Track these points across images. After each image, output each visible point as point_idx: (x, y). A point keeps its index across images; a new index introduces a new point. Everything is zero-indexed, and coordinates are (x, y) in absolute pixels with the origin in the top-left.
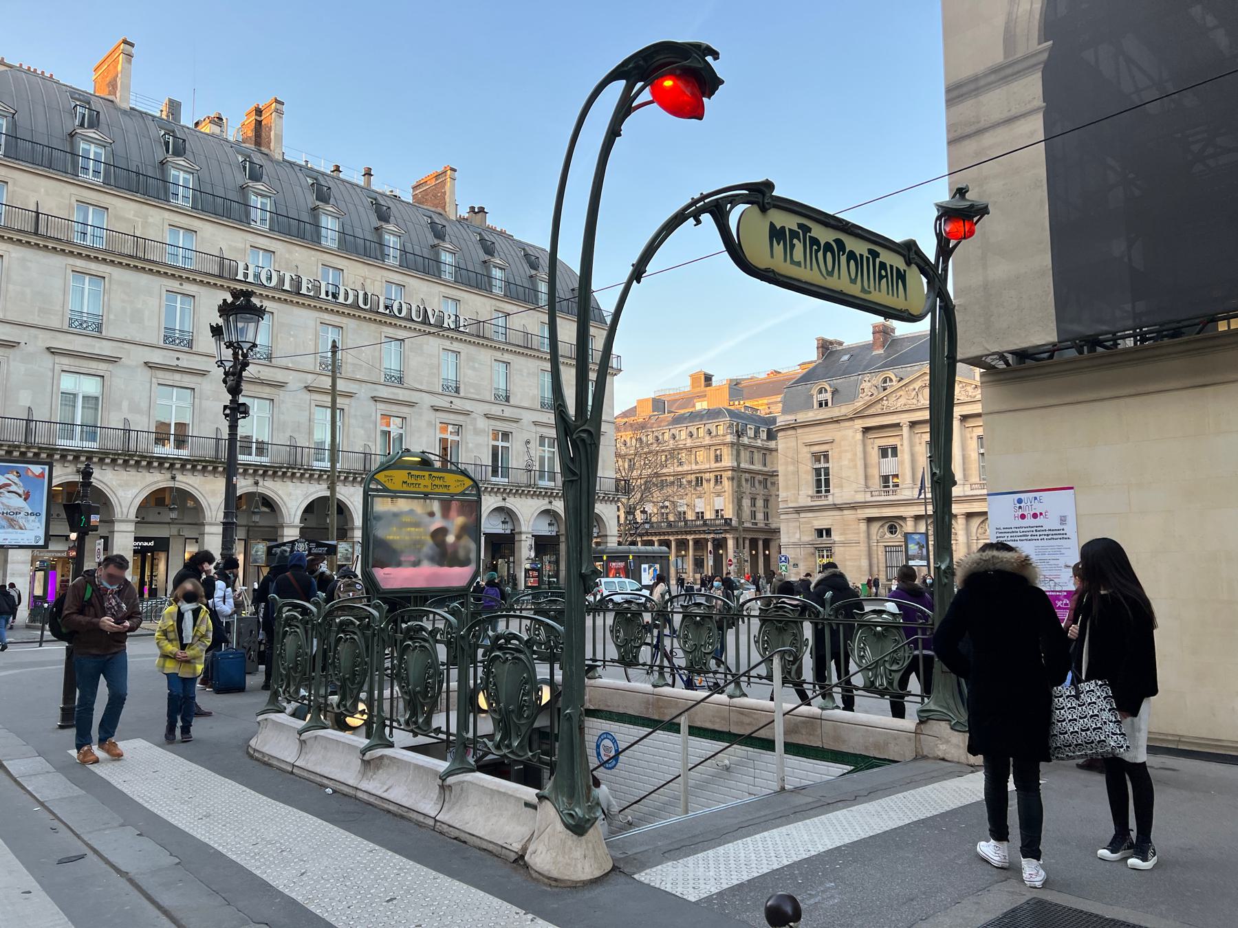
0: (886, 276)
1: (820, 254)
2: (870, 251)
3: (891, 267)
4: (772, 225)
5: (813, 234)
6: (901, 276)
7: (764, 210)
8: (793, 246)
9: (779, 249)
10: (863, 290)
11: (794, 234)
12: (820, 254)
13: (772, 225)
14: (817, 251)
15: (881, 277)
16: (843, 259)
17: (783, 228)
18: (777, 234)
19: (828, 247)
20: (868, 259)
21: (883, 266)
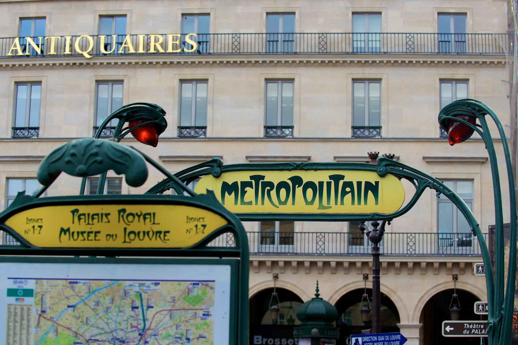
0: (352, 191)
1: (273, 193)
3: (359, 184)
4: (225, 185)
5: (266, 180)
8: (244, 193)
10: (321, 206)
11: (245, 184)
12: (273, 193)
13: (225, 185)
14: (269, 191)
15: (344, 193)
16: (299, 190)
19: (283, 185)
20: (329, 184)
21: (350, 184)
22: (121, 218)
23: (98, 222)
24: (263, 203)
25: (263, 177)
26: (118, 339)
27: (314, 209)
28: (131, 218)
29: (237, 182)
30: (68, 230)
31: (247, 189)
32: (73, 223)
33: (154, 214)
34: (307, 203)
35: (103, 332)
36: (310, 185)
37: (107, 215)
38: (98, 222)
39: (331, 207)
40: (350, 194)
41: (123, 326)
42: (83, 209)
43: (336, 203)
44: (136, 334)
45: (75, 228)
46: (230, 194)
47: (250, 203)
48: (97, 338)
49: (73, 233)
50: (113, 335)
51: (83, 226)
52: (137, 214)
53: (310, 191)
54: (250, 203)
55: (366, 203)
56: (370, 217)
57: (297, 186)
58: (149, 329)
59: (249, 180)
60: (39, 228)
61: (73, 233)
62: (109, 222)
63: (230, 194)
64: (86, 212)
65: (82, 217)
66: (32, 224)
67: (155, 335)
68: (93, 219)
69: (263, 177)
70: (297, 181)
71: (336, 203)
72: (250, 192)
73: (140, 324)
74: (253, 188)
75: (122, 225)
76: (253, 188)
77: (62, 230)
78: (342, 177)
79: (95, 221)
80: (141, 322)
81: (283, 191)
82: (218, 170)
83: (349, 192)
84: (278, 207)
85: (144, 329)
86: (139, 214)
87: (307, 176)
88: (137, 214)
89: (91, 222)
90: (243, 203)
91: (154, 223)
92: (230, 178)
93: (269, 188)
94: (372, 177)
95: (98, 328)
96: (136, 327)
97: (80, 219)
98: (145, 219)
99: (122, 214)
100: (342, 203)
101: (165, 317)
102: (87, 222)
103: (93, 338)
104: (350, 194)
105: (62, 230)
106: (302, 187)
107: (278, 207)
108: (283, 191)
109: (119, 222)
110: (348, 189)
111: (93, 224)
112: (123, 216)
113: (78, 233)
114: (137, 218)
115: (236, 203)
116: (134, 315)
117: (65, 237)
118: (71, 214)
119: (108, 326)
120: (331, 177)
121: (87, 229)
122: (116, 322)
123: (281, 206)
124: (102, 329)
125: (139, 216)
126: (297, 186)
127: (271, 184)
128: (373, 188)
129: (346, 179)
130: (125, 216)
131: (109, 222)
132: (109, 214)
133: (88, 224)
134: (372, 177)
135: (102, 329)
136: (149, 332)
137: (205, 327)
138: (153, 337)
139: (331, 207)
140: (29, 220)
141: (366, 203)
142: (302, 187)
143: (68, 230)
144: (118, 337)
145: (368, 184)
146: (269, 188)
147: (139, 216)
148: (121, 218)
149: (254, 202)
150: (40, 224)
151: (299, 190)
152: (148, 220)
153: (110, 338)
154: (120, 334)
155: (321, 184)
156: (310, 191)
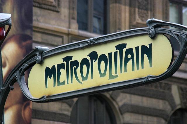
0: (132, 58)
1: (78, 70)
2: (117, 47)
3: (137, 48)
5: (73, 59)
6: (147, 51)
7: (41, 63)
8: (59, 74)
9: (51, 80)
10: (111, 77)
11: (61, 66)
12: (78, 70)
14: (75, 69)
15: (127, 60)
16: (95, 64)
17: (54, 66)
18: (49, 72)
19: (85, 61)
20: (116, 53)
21: (130, 51)
24: (72, 82)
25: (71, 58)
27: (105, 81)
29: (54, 66)
31: (62, 70)
34: (102, 75)
36: (103, 57)
39: (117, 76)
40: (131, 60)
43: (121, 72)
46: (50, 78)
47: (63, 83)
53: (103, 63)
54: (63, 83)
55: (143, 67)
56: (145, 80)
57: (94, 60)
59: (61, 62)
63: (50, 78)
69: (71, 58)
70: (93, 55)
71: (121, 72)
72: (63, 71)
74: (65, 69)
76: (65, 69)
78: (124, 45)
81: (85, 67)
82: (39, 58)
83: (130, 59)
84: (81, 83)
87: (101, 51)
90: (59, 84)
92: (50, 63)
93: (75, 67)
94: (145, 41)
100: (126, 71)
104: (131, 60)
106: (97, 61)
107: (81, 83)
108: (85, 67)
110: (129, 56)
115: (54, 85)
120: (117, 47)
123: (84, 82)
126: (94, 60)
127: (76, 63)
128: (147, 51)
129: (128, 47)
134: (145, 41)
139: (117, 76)
141: (143, 67)
142: (97, 61)
145: (144, 47)
146: (75, 67)
149: (66, 82)
151: (95, 64)
155: (110, 54)
156: (103, 63)
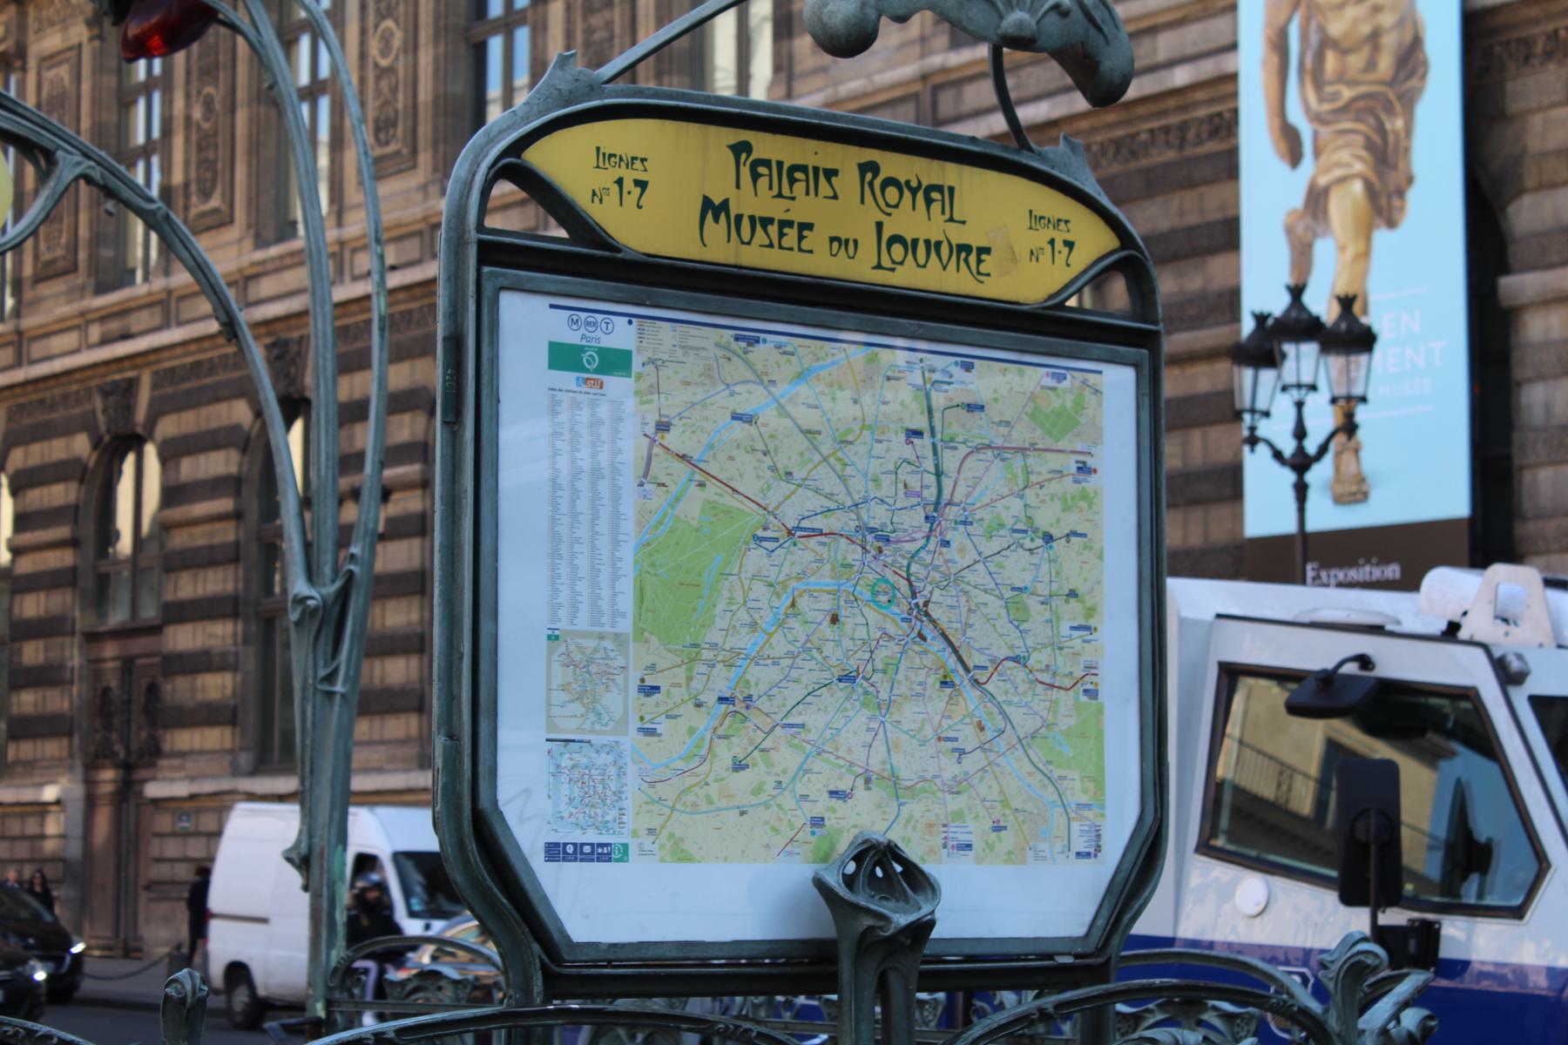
22: (867, 188)
23: (807, 193)
26: (872, 530)
28: (892, 193)
30: (725, 205)
32: (738, 186)
33: (951, 190)
35: (833, 506)
37: (831, 174)
38: (807, 193)
41: (886, 489)
42: (766, 146)
44: (918, 517)
45: (753, 200)
48: (818, 523)
49: (739, 218)
50: (859, 517)
51: (753, 200)
52: (908, 182)
58: (949, 503)
60: (638, 190)
61: (739, 218)
62: (835, 197)
64: (774, 157)
65: (762, 170)
66: (616, 173)
67: (965, 523)
68: (792, 181)
73: (928, 487)
75: (872, 213)
77: (707, 204)
79: (799, 188)
80: (931, 479)
85: (937, 503)
86: (914, 184)
88: (908, 182)
89: (786, 191)
91: (951, 219)
95: (817, 491)
96: (919, 495)
97: (755, 177)
98: (929, 202)
99: (869, 176)
101: (987, 469)
102: (775, 191)
103: (804, 524)
105: (707, 204)
109: (862, 202)
111: (793, 199)
112: (871, 184)
113: (752, 219)
114: (907, 195)
116: (913, 458)
117: (716, 230)
118: (730, 155)
119: (846, 487)
121: (777, 209)
122: (865, 475)
124: (829, 496)
125: (914, 191)
130: (877, 183)
131: (835, 197)
132: (834, 172)
133: (780, 195)
135: (829, 496)
136: (952, 513)
137: (1083, 504)
138: (961, 528)
140: (605, 158)
143: (725, 205)
144: (872, 524)
147: (914, 191)
148: (867, 188)
150: (642, 177)
152: (936, 207)
153: (853, 524)
154: (877, 516)
